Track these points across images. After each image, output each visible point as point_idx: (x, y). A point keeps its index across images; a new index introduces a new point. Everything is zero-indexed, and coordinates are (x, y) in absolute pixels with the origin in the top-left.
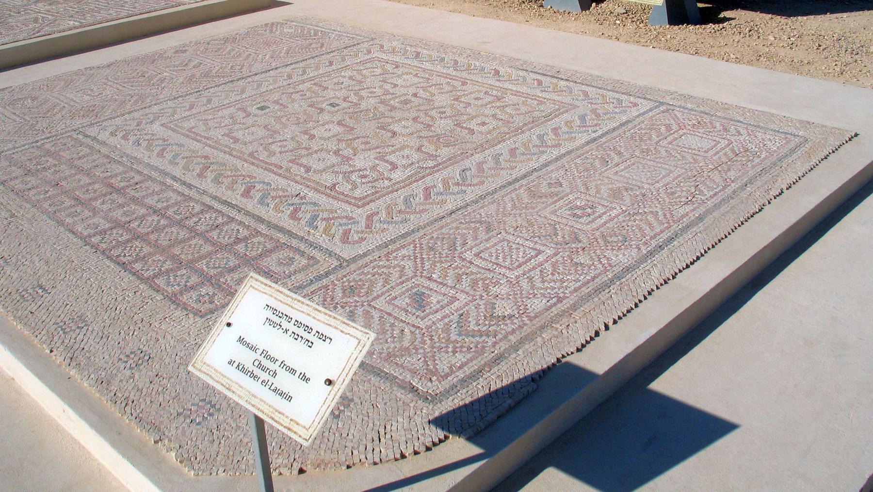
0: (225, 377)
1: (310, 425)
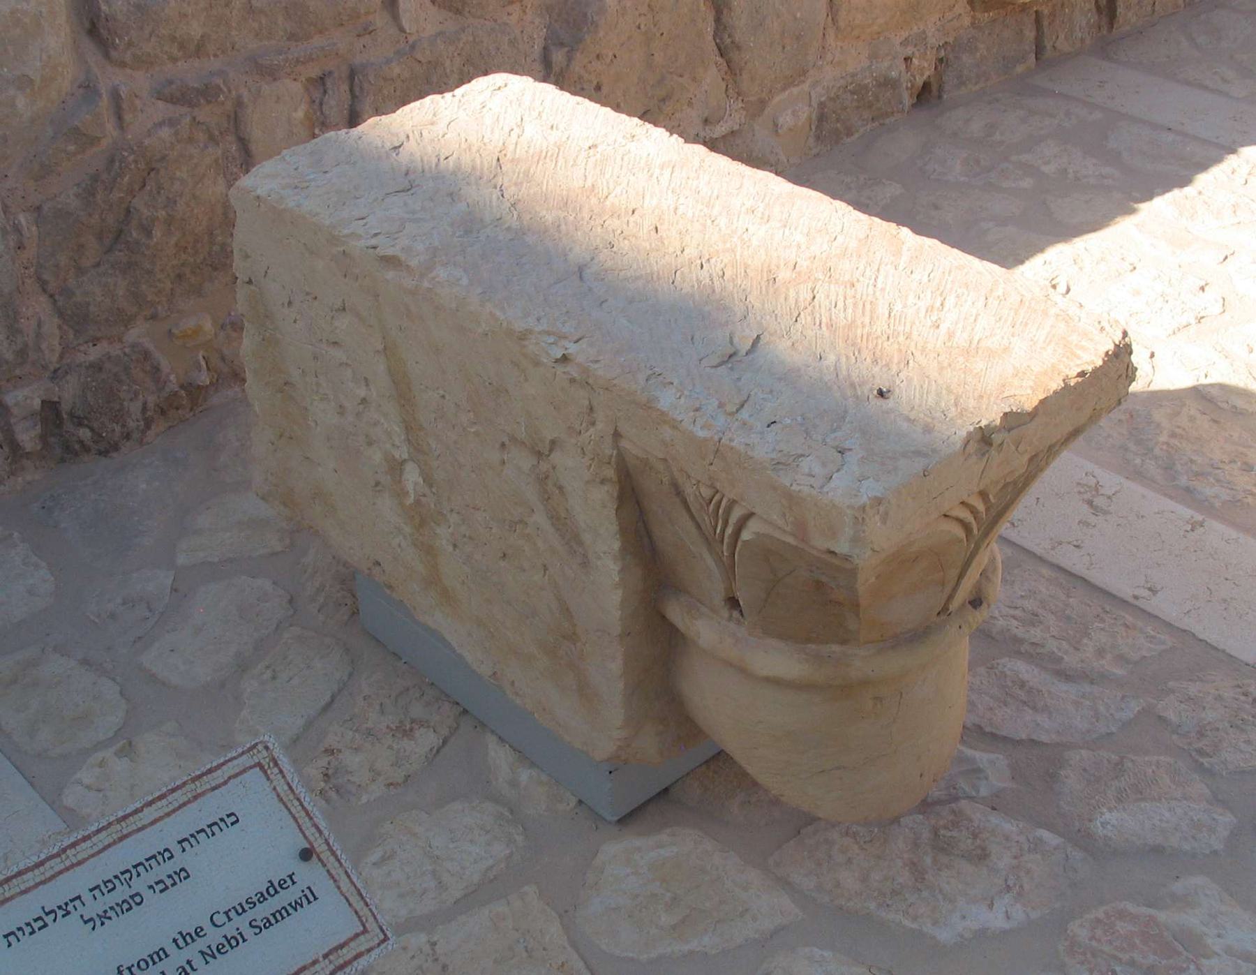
1: (359, 924)
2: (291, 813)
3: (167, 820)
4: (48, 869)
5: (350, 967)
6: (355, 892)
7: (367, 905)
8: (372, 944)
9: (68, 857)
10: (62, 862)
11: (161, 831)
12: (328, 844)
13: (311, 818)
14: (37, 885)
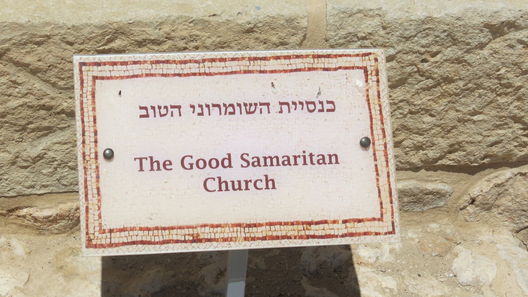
0: (173, 228)
1: (380, 212)
2: (370, 113)
3: (283, 74)
5: (358, 237)
6: (387, 189)
10: (199, 68)
12: (385, 147)
13: (382, 123)
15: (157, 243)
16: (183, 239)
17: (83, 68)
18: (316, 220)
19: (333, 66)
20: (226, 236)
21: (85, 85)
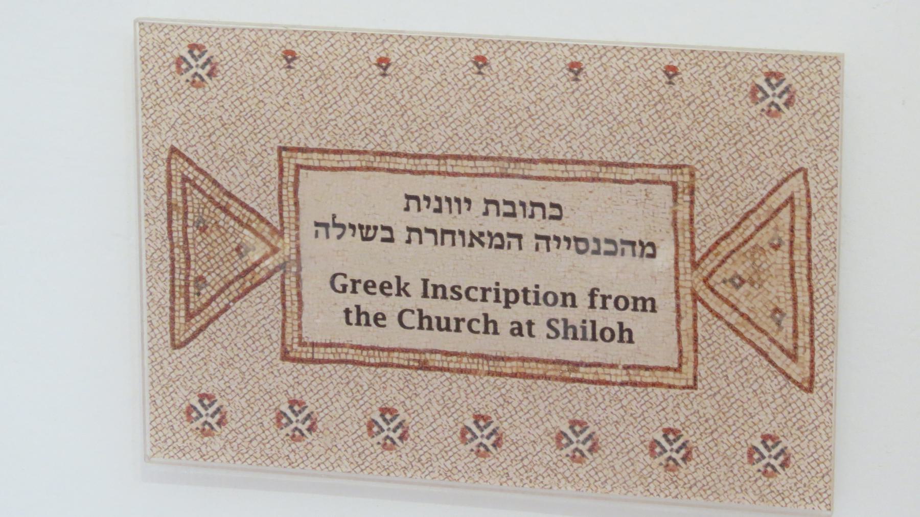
0: (393, 350)
3: (553, 183)
4: (421, 165)
7: (696, 351)
8: (677, 383)
9: (445, 164)
11: (591, 192)
14: (405, 171)
15: (372, 365)
16: (406, 363)
17: (284, 154)
18: (587, 361)
19: (628, 178)
20: (463, 366)
21: (285, 174)
